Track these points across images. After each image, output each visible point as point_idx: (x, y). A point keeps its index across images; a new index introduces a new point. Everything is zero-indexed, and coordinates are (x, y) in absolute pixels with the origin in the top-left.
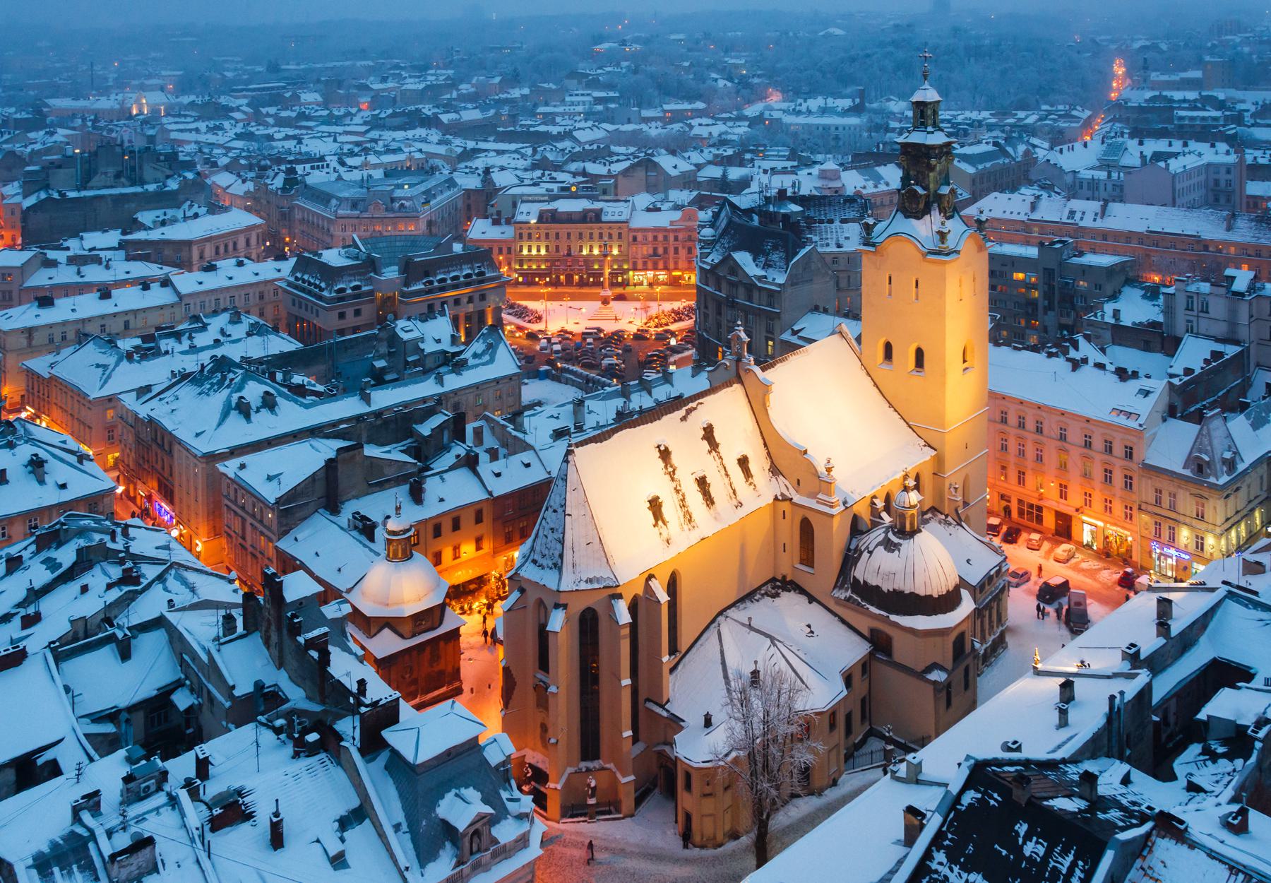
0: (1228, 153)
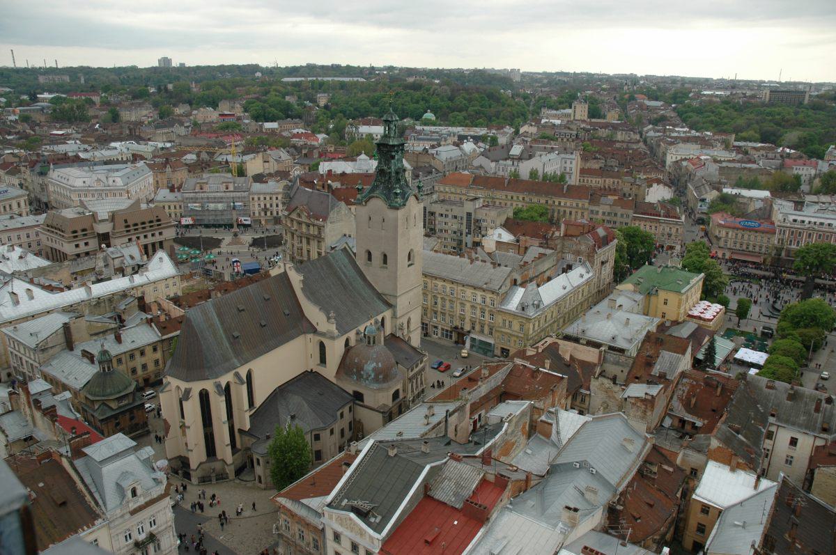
0: (572, 153)
